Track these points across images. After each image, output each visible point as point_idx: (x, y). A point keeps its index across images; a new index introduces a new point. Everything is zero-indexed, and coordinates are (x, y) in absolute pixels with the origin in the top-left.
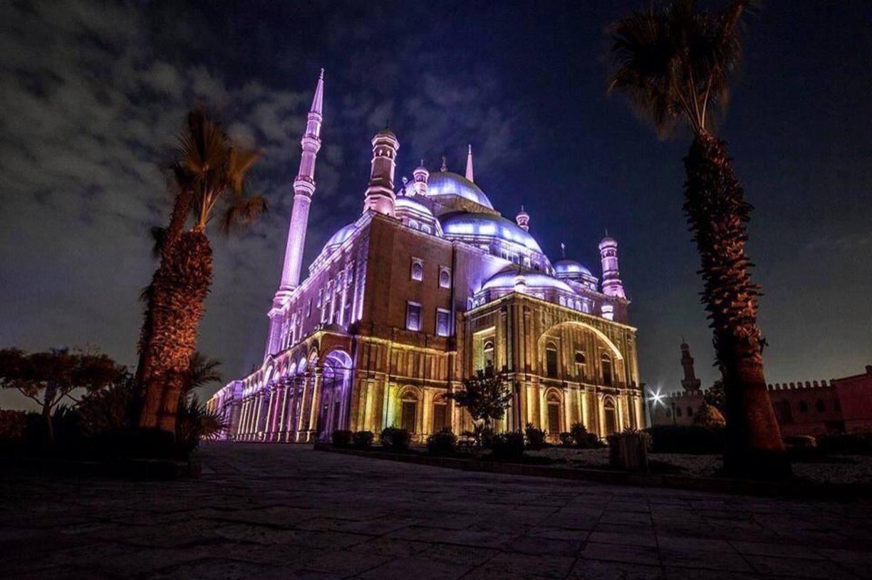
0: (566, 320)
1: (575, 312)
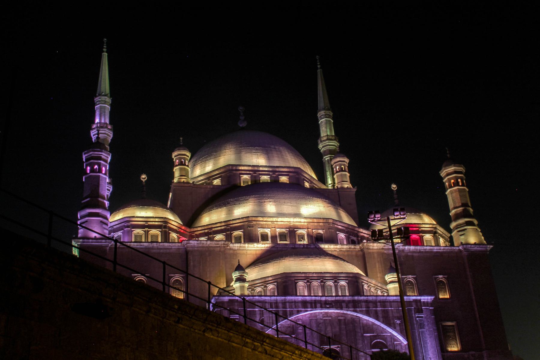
0: (298, 312)
1: (313, 298)
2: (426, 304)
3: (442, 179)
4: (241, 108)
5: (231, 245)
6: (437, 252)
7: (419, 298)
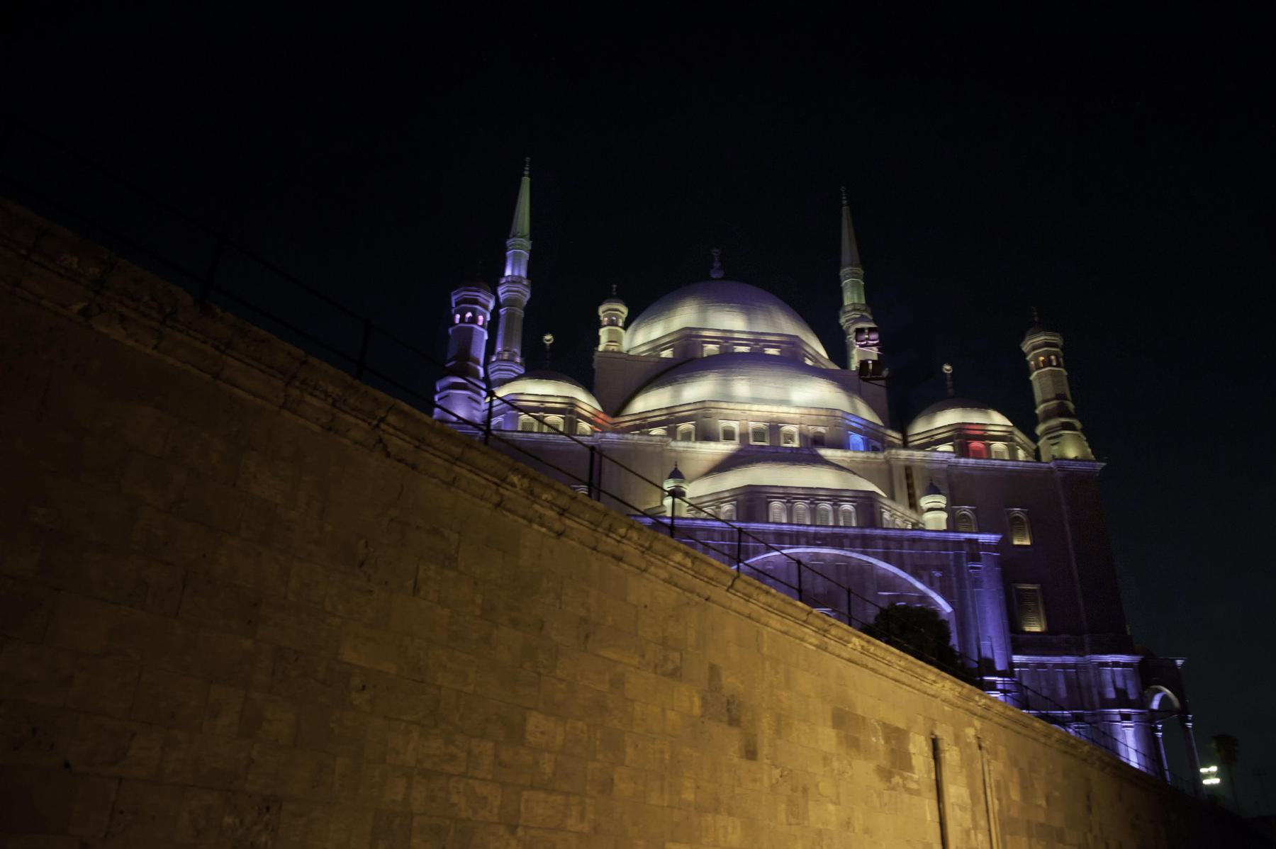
1: (795, 528)
2: (987, 546)
3: (1025, 355)
5: (673, 444)
6: (1011, 471)
7: (975, 536)
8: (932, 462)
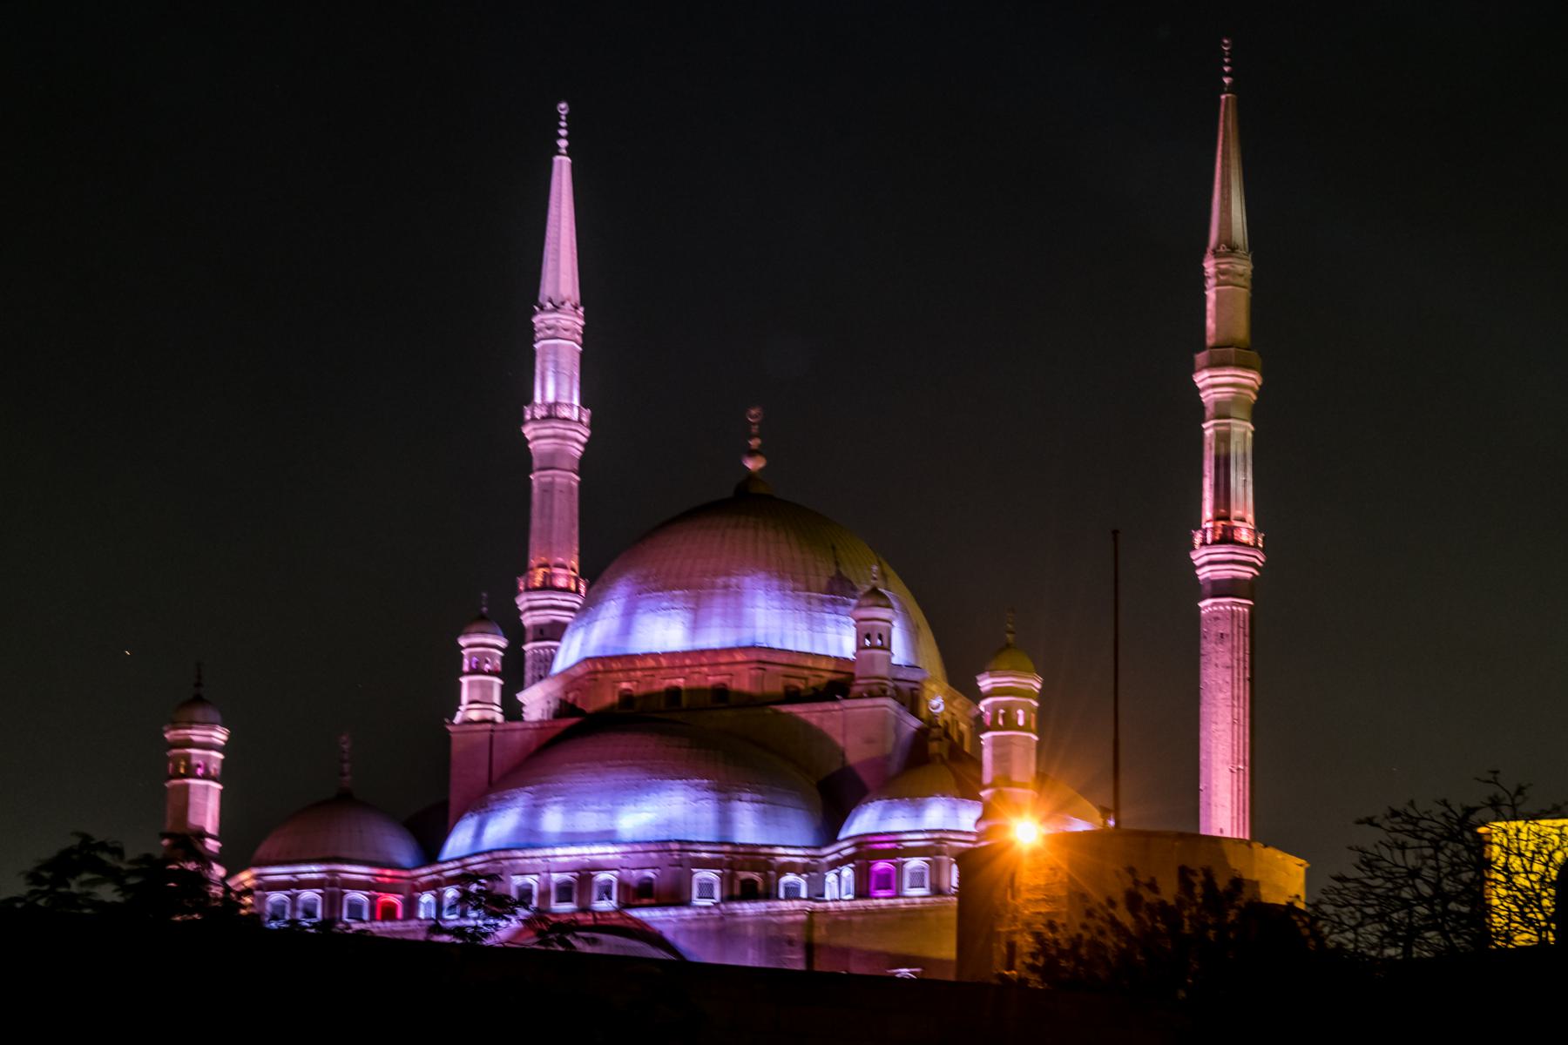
4: (753, 412)
8: (781, 913)
